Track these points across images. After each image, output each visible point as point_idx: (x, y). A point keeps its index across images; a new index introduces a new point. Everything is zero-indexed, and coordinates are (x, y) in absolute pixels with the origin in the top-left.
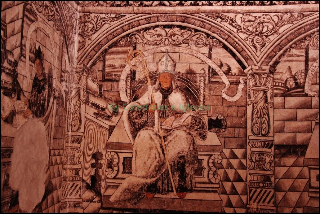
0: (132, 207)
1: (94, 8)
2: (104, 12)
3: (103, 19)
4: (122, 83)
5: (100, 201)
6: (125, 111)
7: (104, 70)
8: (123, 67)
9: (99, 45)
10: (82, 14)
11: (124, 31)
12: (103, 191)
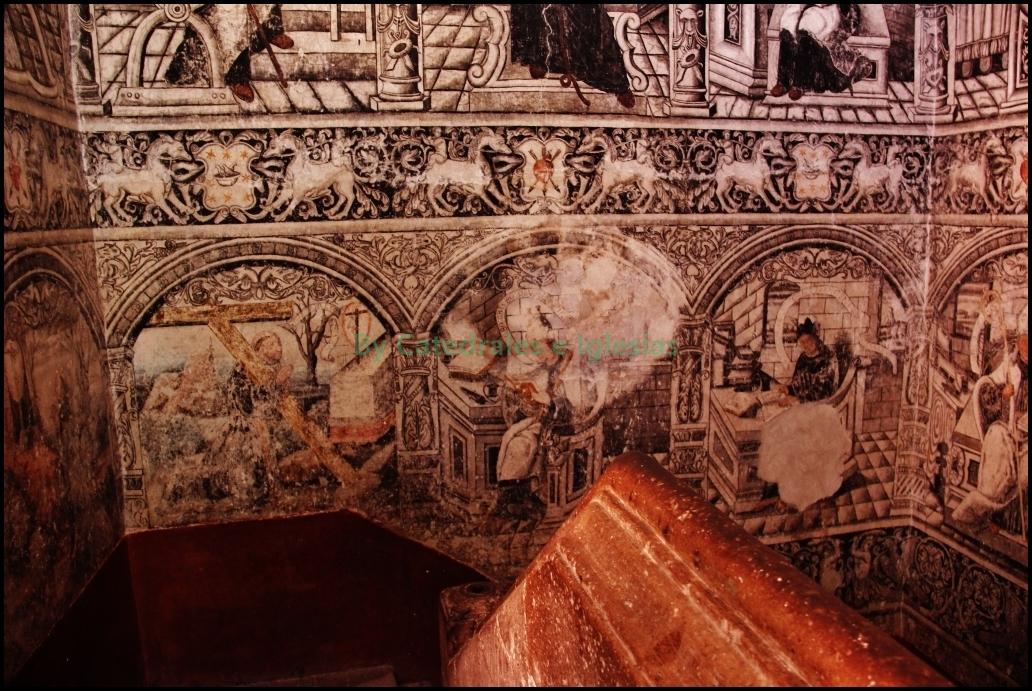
0: (974, 537)
1: (946, 217)
2: (957, 223)
3: (956, 236)
4: (974, 342)
5: (943, 513)
6: (975, 387)
7: (955, 318)
8: (976, 316)
9: (952, 276)
10: (932, 226)
11: (980, 256)
12: (946, 500)
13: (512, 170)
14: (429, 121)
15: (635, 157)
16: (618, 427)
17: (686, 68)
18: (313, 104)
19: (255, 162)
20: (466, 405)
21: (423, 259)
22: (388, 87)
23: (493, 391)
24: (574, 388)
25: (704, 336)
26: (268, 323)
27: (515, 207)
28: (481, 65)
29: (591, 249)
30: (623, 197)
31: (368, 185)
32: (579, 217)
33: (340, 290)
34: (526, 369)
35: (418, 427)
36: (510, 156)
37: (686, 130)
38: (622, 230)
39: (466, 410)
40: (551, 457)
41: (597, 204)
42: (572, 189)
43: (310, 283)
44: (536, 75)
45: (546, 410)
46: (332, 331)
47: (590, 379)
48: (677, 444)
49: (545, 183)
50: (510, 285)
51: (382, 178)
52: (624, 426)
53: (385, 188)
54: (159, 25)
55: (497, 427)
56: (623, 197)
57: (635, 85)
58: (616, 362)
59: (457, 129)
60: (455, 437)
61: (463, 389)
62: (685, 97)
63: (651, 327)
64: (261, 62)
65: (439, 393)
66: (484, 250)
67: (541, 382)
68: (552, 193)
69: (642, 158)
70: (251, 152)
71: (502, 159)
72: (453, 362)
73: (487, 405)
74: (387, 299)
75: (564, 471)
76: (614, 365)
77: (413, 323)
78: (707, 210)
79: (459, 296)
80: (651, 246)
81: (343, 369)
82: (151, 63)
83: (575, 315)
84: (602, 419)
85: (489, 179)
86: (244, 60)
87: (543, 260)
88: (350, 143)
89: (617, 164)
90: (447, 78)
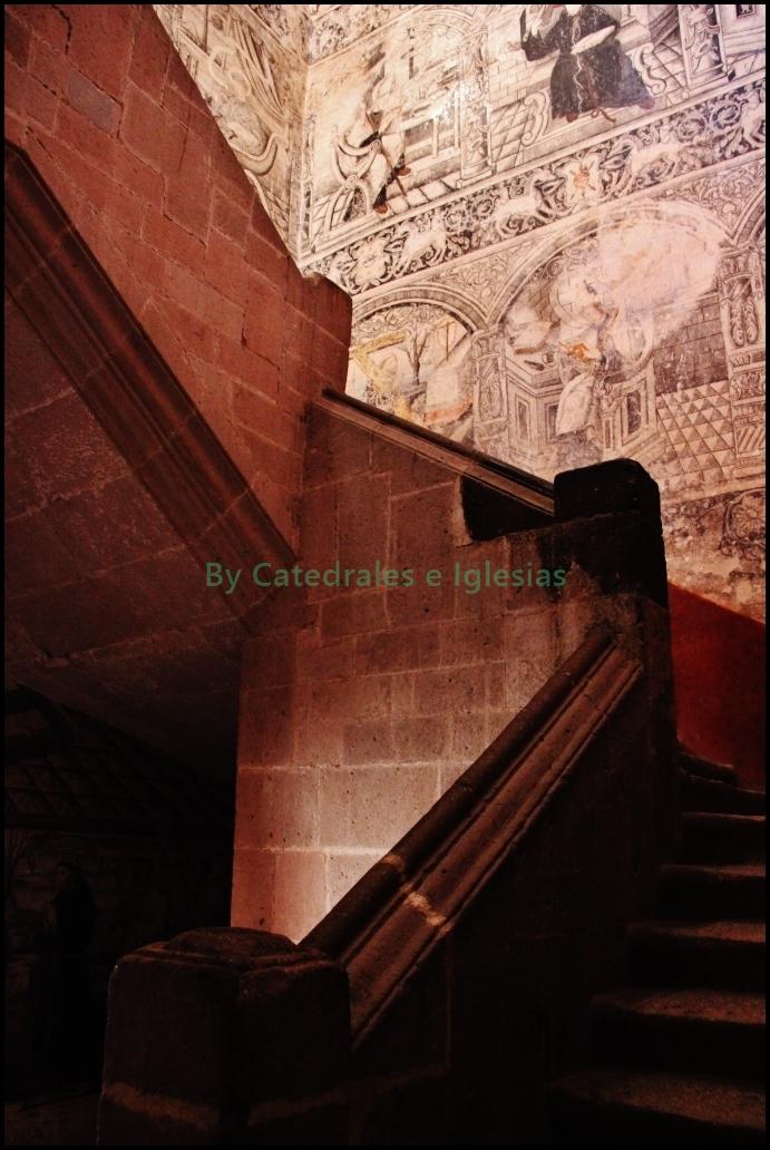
13: (557, 189)
14: (497, 180)
15: (659, 141)
16: (669, 365)
17: (700, 58)
18: (423, 199)
19: (386, 246)
20: (529, 374)
21: (494, 273)
22: (468, 171)
23: (550, 359)
24: (623, 341)
25: (750, 260)
26: (390, 348)
27: (561, 214)
28: (530, 131)
29: (627, 222)
30: (651, 174)
31: (456, 235)
32: (615, 203)
33: (437, 312)
34: (577, 332)
35: (490, 400)
36: (555, 180)
37: (706, 102)
38: (653, 198)
39: (529, 379)
40: (604, 405)
41: (629, 187)
42: (605, 184)
43: (417, 313)
44: (570, 121)
45: (598, 364)
46: (430, 343)
47: (637, 328)
48: (737, 369)
49: (583, 188)
50: (559, 273)
51: (464, 228)
52: (675, 363)
53: (468, 234)
54: (342, 194)
55: (555, 387)
56: (651, 174)
57: (654, 89)
58: (660, 307)
59: (515, 178)
60: (520, 403)
61: (526, 362)
62: (701, 79)
63: (692, 267)
64: (393, 188)
65: (507, 369)
66: (539, 253)
67: (591, 341)
68: (589, 193)
69: (664, 140)
70: (384, 242)
71: (549, 185)
72: (516, 342)
73: (546, 370)
74: (469, 310)
75: (618, 416)
76: (658, 310)
77: (486, 320)
78: (736, 154)
79: (521, 291)
80: (682, 202)
81: (437, 367)
82: (336, 216)
83: (617, 278)
84: (651, 361)
85: (540, 201)
86: (383, 191)
87: (587, 244)
88: (443, 213)
89: (644, 152)
90: (507, 149)
